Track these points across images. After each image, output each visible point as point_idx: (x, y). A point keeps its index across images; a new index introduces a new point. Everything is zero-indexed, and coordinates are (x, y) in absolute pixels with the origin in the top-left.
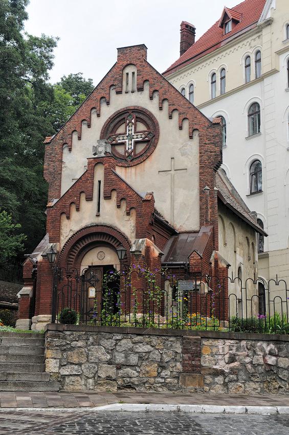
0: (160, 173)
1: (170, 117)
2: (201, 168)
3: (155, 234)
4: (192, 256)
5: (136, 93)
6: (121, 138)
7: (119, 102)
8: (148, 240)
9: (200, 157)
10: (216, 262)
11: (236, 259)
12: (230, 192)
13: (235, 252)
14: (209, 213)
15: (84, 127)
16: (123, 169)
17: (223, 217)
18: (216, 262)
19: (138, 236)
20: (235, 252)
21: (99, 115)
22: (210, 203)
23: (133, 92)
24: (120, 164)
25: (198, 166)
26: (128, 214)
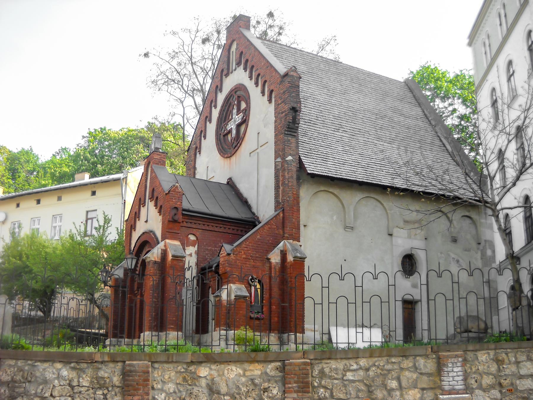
0: (252, 154)
1: (257, 84)
2: (276, 135)
3: (198, 233)
4: (221, 253)
5: (238, 69)
6: (229, 125)
7: (229, 84)
8: (167, 241)
9: (276, 122)
10: (284, 254)
11: (392, 244)
12: (450, 155)
13: (391, 235)
14: (281, 192)
15: (208, 123)
16: (228, 159)
17: (336, 191)
18: (284, 254)
19: (163, 239)
20: (391, 235)
21: (215, 107)
22: (281, 178)
23: (235, 70)
24: (226, 156)
25: (273, 134)
26: (160, 212)
